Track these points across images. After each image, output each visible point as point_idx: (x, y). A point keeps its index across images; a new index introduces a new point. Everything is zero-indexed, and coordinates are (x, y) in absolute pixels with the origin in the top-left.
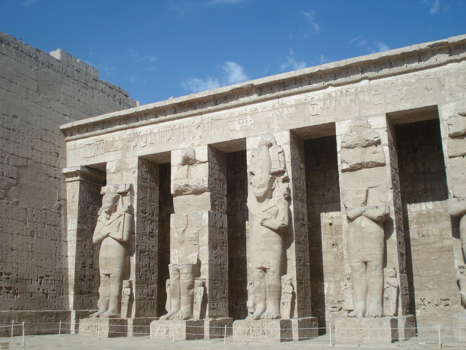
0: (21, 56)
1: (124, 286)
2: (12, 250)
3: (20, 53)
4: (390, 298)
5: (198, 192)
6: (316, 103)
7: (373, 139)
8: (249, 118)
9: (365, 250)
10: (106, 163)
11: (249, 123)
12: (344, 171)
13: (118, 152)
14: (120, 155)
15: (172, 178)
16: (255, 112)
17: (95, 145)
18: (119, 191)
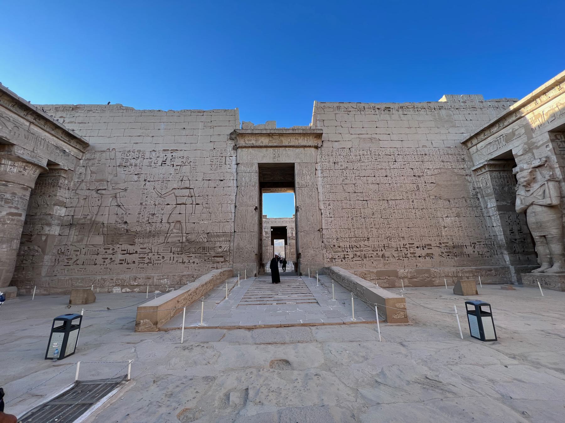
3: (416, 109)
10: (511, 150)
13: (522, 137)
17: (496, 141)
18: (533, 166)
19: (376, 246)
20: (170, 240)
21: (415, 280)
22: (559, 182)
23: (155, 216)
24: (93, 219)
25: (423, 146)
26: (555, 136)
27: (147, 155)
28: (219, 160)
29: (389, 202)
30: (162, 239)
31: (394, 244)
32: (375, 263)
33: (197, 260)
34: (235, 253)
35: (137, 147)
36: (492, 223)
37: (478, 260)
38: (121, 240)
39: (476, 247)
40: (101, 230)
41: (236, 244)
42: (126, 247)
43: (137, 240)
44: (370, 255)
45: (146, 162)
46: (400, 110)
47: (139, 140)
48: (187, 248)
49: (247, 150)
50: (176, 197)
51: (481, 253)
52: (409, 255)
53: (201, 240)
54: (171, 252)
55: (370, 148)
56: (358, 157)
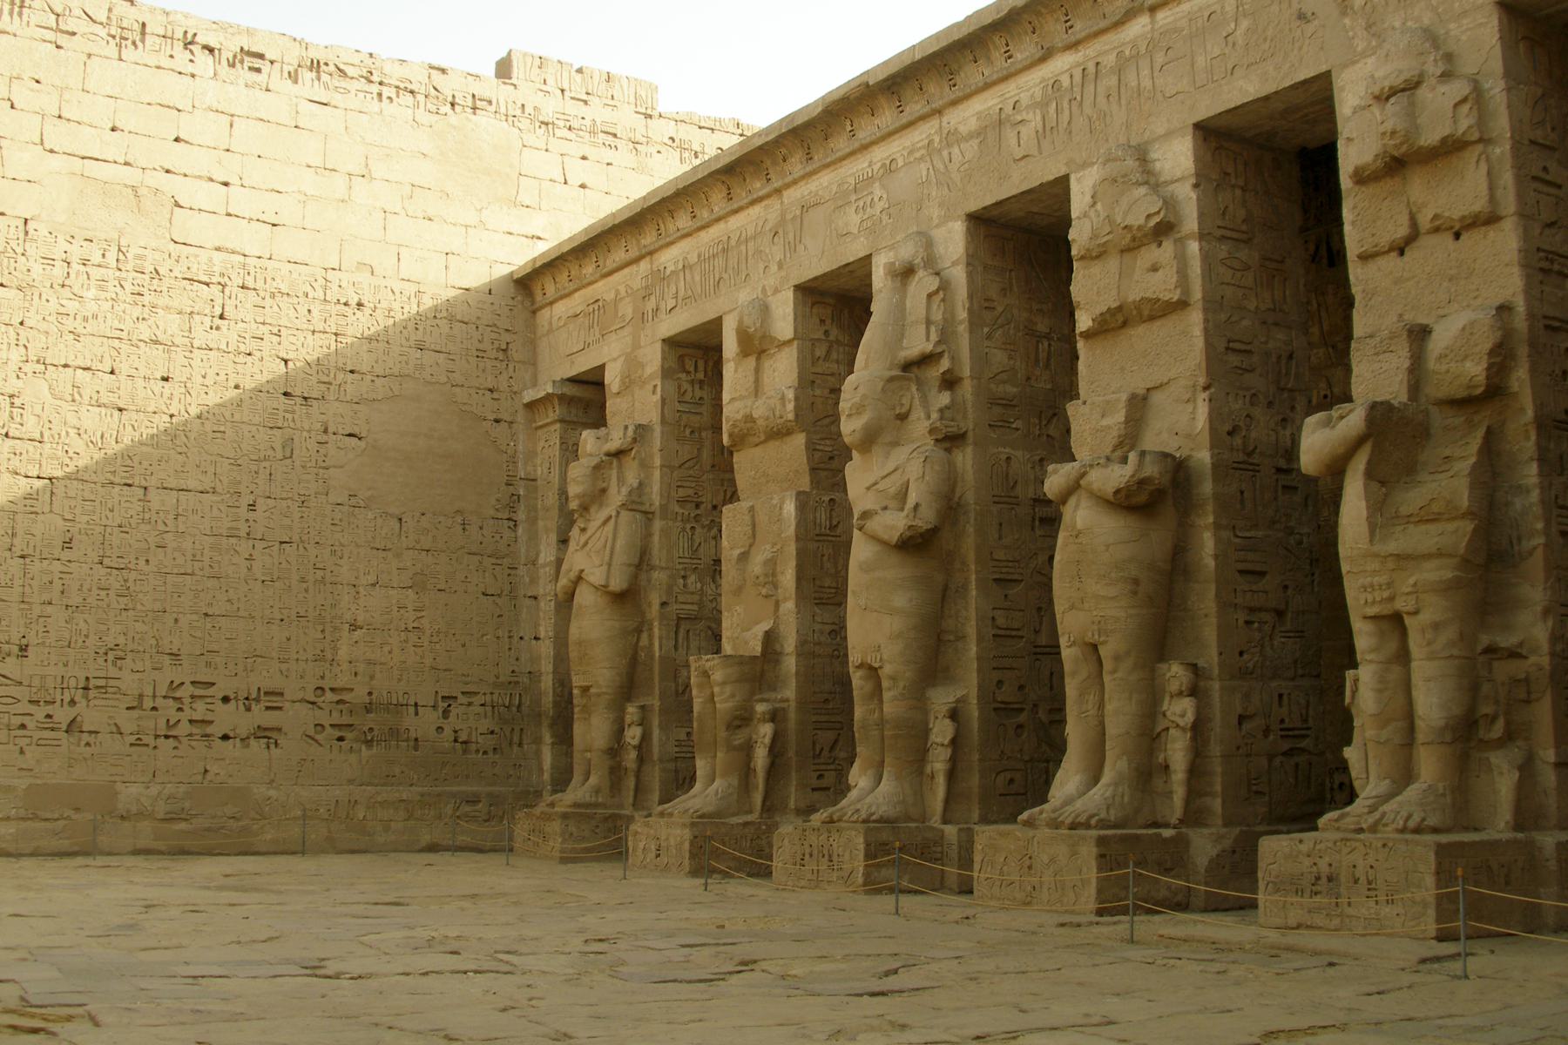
0: (380, 95)
1: (628, 719)
2: (354, 627)
3: (375, 88)
4: (1172, 767)
5: (778, 433)
6: (1024, 116)
7: (1142, 221)
8: (878, 191)
9: (1086, 605)
10: (602, 367)
11: (879, 206)
12: (1087, 335)
14: (629, 339)
15: (726, 397)
16: (889, 168)
19: (50, 683)
21: (183, 826)
22: (648, 515)
25: (361, 265)
26: (681, 358)
29: (152, 494)
31: (129, 682)
32: (32, 753)
36: (537, 625)
37: (444, 764)
39: (454, 711)
44: (17, 721)
46: (307, 76)
51: (463, 737)
52: (184, 729)
55: (121, 234)
56: (59, 270)
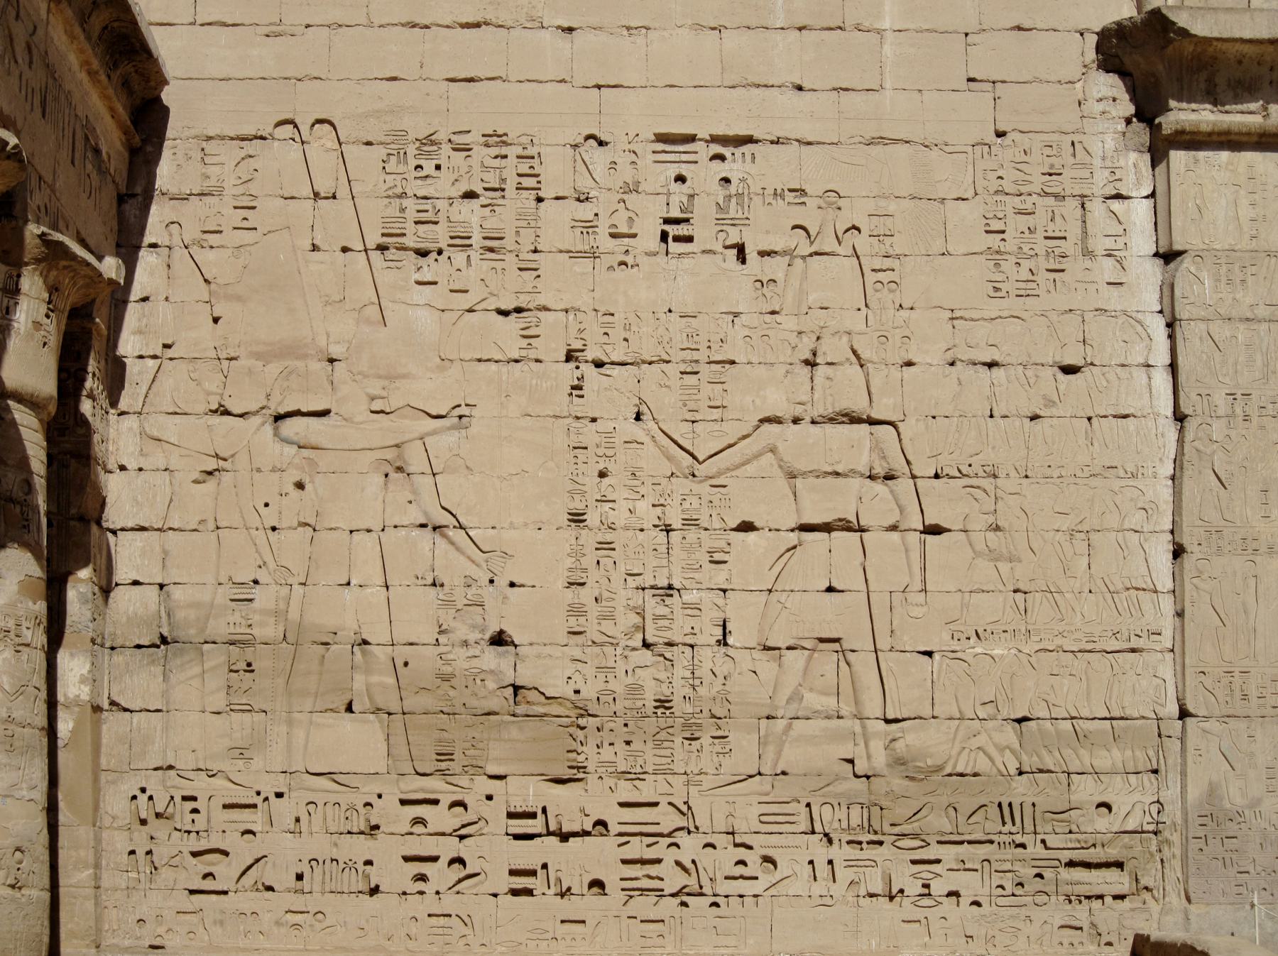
20: (792, 757)
23: (675, 601)
24: (294, 614)
27: (556, 173)
28: (1040, 220)
30: (744, 749)
33: (969, 884)
34: (1194, 845)
35: (475, 112)
38: (496, 750)
40: (359, 681)
41: (1194, 793)
42: (529, 793)
43: (590, 749)
45: (557, 223)
47: (476, 52)
48: (902, 811)
49: (1225, 155)
50: (792, 476)
53: (982, 764)
54: (813, 832)
